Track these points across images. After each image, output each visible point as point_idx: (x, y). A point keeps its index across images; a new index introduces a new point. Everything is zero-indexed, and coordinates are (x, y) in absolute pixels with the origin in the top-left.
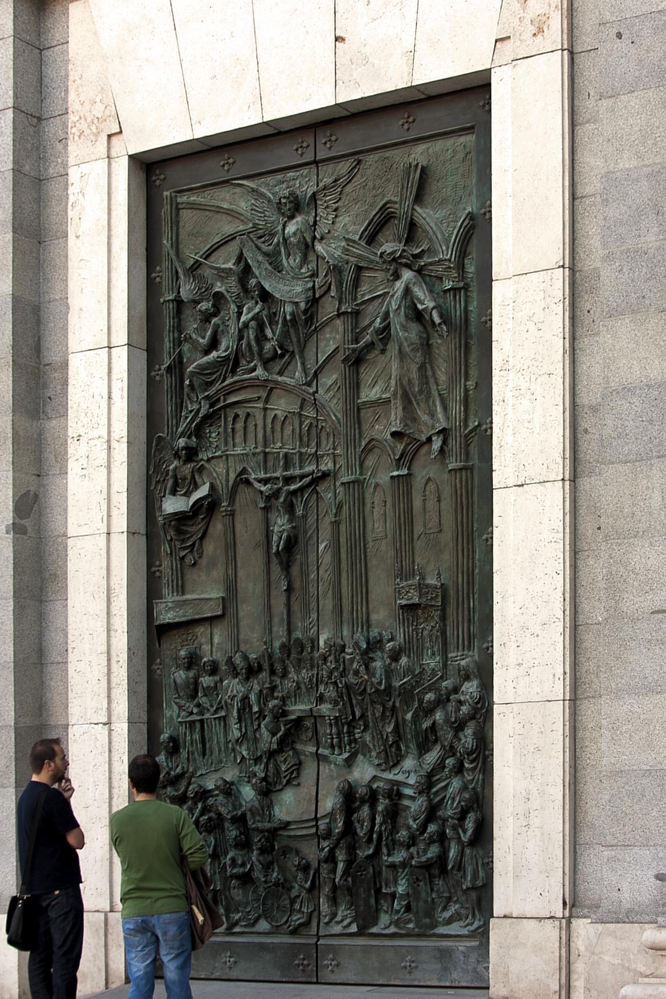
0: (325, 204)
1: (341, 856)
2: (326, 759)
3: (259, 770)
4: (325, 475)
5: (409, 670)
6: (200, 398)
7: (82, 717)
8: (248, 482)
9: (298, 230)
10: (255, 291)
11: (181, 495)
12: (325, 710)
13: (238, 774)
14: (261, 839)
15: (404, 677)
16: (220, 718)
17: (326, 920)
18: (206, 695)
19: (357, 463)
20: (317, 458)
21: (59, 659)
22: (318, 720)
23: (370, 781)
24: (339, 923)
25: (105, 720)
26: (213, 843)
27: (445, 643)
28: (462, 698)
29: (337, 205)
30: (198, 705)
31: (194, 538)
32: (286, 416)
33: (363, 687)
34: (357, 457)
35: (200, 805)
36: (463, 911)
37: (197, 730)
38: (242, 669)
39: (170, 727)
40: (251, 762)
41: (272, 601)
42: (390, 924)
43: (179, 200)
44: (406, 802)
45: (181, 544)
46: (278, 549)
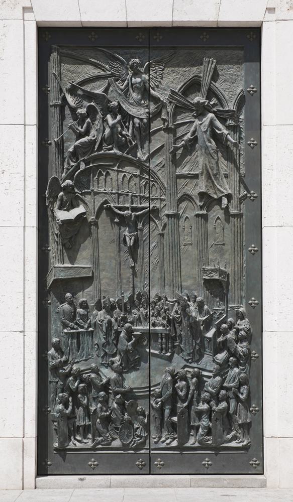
4: (155, 212)
5: (208, 312)
8: (109, 209)
9: (142, 80)
11: (64, 210)
17: (155, 440)
19: (176, 205)
24: (163, 442)
25: (22, 330)
28: (240, 327)
29: (162, 72)
30: (76, 324)
43: (61, 50)
44: (205, 379)
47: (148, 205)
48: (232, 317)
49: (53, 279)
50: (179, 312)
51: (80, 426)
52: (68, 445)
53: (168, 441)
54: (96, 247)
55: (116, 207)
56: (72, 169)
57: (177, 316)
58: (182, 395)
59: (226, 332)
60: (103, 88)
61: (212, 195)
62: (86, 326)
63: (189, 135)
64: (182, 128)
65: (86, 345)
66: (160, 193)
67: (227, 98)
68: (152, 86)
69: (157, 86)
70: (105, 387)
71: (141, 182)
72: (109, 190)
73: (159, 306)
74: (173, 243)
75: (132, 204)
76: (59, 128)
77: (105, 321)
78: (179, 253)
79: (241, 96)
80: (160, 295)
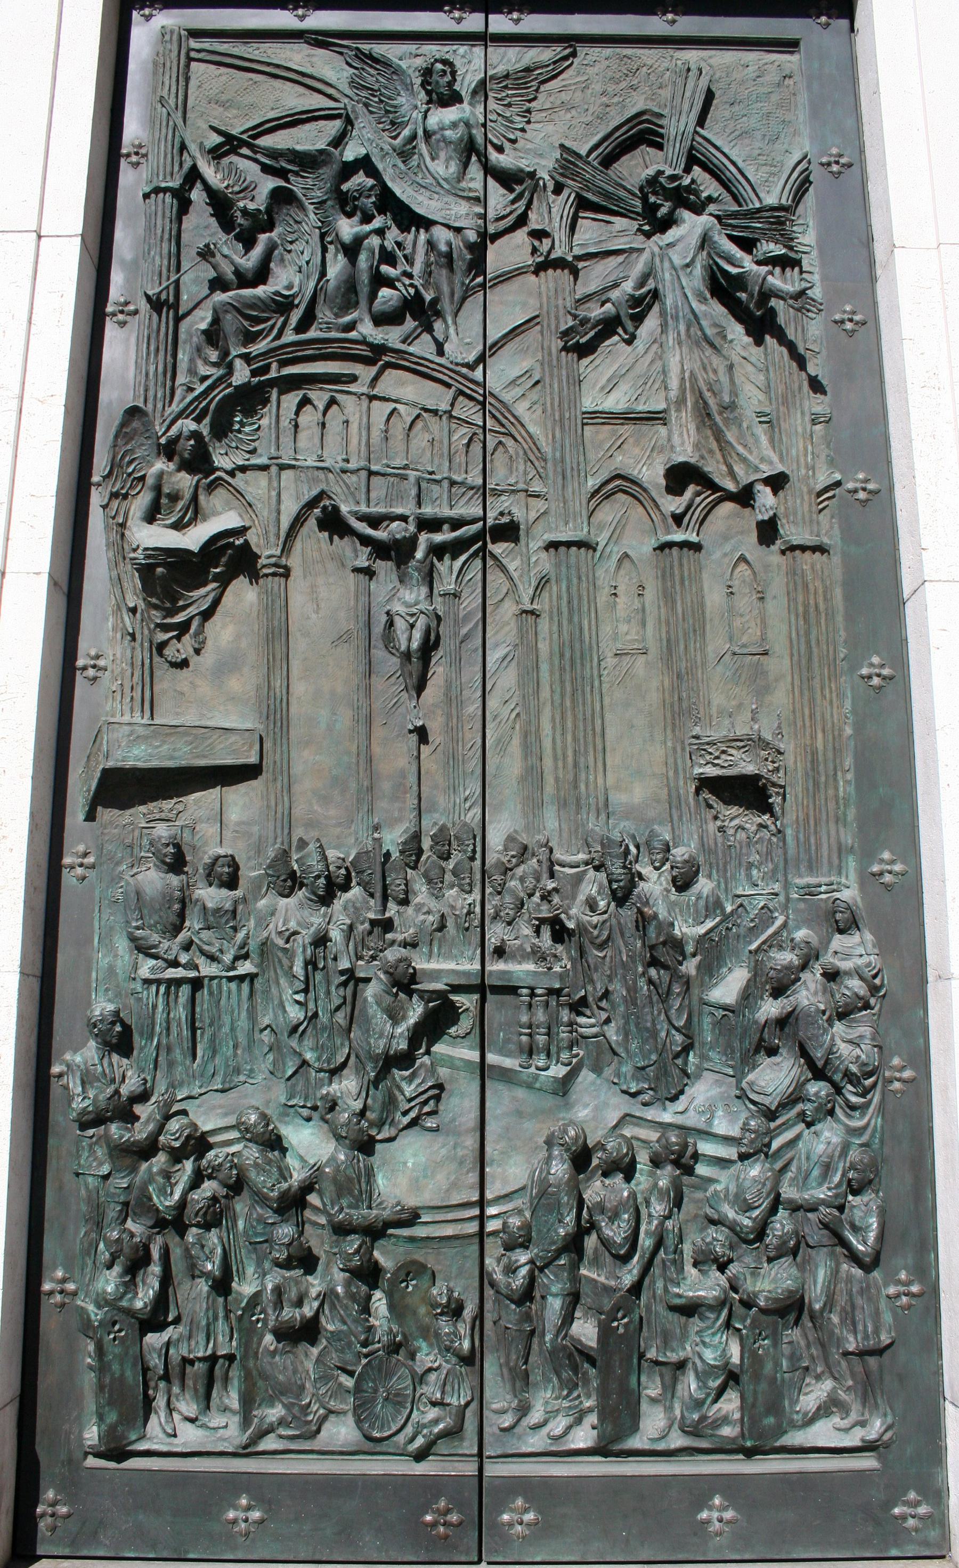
2: (506, 1075)
5: (713, 906)
6: (234, 353)
9: (460, 120)
10: (369, 196)
11: (167, 526)
12: (522, 975)
13: (283, 1100)
14: (360, 1247)
15: (706, 917)
16: (241, 978)
17: (507, 1421)
26: (219, 1250)
28: (845, 965)
31: (192, 610)
32: (418, 416)
33: (606, 933)
34: (584, 502)
35: (189, 1165)
38: (318, 877)
41: (377, 749)
45: (165, 618)
47: (481, 512)
48: (808, 923)
49: (101, 767)
50: (602, 904)
51: (192, 1362)
52: (142, 1437)
53: (558, 1425)
54: (278, 657)
55: (362, 518)
57: (595, 919)
61: (717, 480)
62: (227, 958)
65: (226, 1029)
66: (526, 473)
69: (514, 142)
71: (455, 438)
73: (522, 880)
74: (577, 646)
76: (165, 262)
77: (306, 936)
78: (596, 683)
80: (524, 838)
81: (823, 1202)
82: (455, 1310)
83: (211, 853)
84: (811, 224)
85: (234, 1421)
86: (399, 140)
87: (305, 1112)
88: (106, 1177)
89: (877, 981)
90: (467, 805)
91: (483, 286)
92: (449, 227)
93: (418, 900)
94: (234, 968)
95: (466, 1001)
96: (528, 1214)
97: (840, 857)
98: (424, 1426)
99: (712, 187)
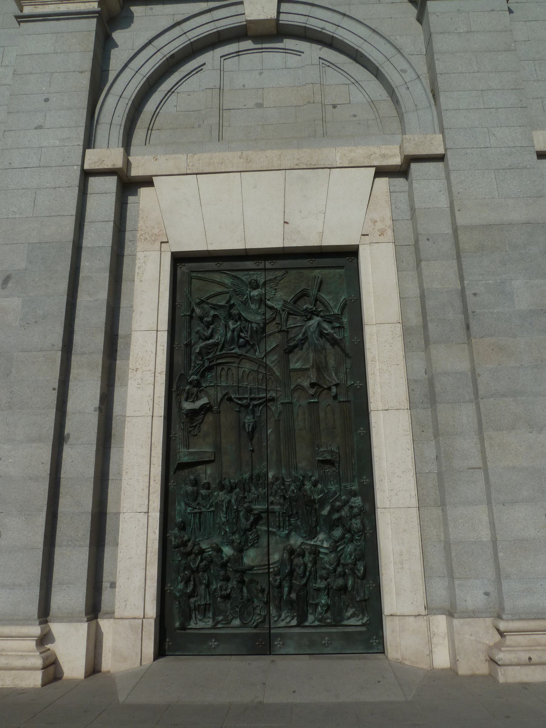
0: (271, 286)
1: (286, 585)
2: (274, 533)
3: (236, 537)
4: (273, 400)
5: (322, 491)
7: (130, 509)
8: (230, 399)
9: (259, 294)
10: (237, 316)
11: (190, 402)
13: (221, 541)
14: (240, 576)
15: (320, 494)
17: (276, 619)
18: (203, 499)
20: (266, 390)
21: (114, 478)
22: (270, 514)
23: (300, 545)
24: (283, 620)
26: (207, 578)
27: (340, 479)
28: (353, 505)
29: (276, 287)
31: (197, 422)
32: (250, 371)
33: (296, 499)
34: (290, 392)
35: (199, 557)
36: (357, 612)
37: (197, 517)
38: (228, 487)
39: (179, 516)
40: (230, 534)
42: (315, 620)
43: (192, 275)
44: (321, 556)
46: (249, 430)
49: (177, 463)
50: (295, 491)
51: (201, 605)
53: (288, 619)
55: (237, 398)
56: (197, 367)
57: (294, 495)
58: (300, 573)
59: (339, 510)
60: (225, 301)
61: (322, 385)
62: (208, 506)
63: (300, 336)
64: (294, 330)
66: (276, 385)
67: (332, 305)
68: (267, 298)
70: (224, 565)
72: (230, 383)
73: (277, 486)
75: (251, 394)
76: (187, 334)
79: (344, 303)
81: (350, 563)
82: (263, 591)
83: (203, 482)
84: (347, 316)
85: (211, 620)
86: (243, 299)
87: (227, 544)
88: (180, 561)
89: (362, 509)
90: (264, 467)
91: (265, 336)
92: (256, 323)
93: (252, 491)
94: (209, 509)
95: (264, 515)
96: (279, 567)
97: (353, 478)
98: (256, 620)
99: (322, 307)
